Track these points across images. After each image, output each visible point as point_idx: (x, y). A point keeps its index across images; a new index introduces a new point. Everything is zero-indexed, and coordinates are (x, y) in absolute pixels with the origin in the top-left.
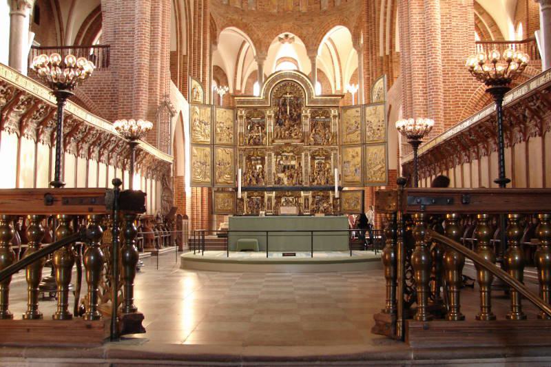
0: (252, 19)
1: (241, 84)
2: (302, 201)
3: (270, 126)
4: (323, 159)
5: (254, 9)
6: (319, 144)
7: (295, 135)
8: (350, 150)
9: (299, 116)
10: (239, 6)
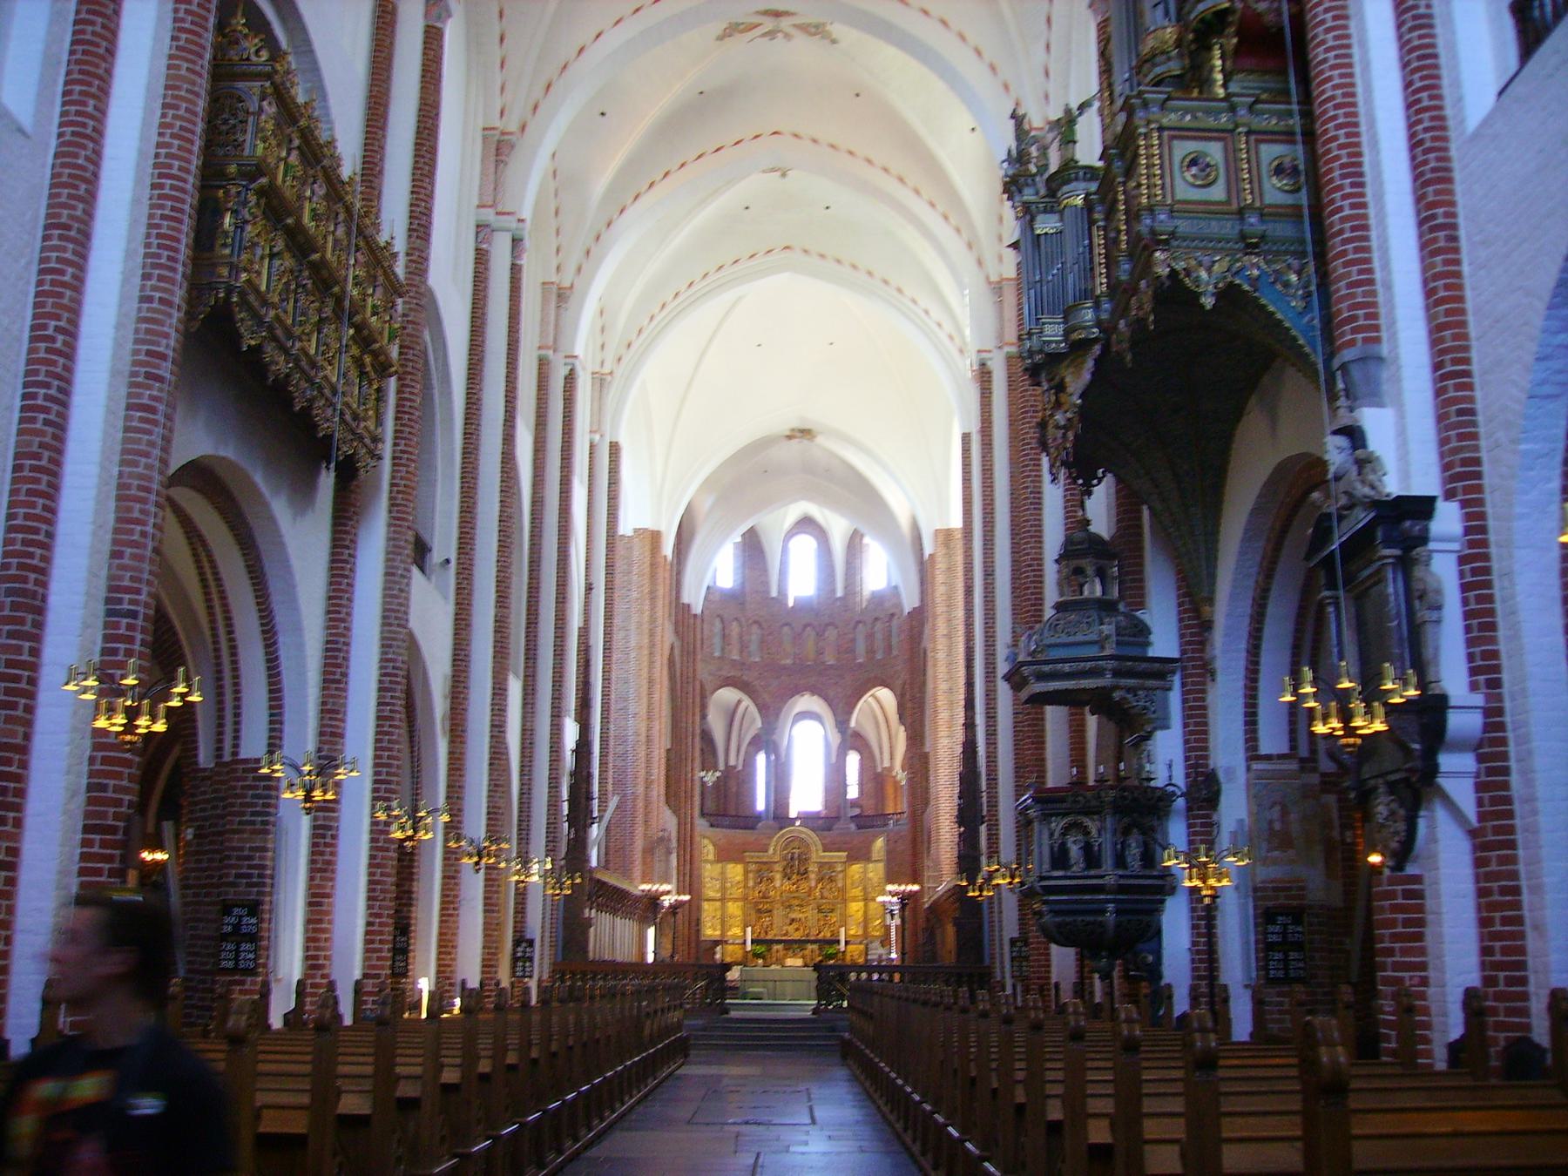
1: (738, 755)
3: (778, 883)
5: (757, 660)
9: (806, 872)
10: (736, 657)
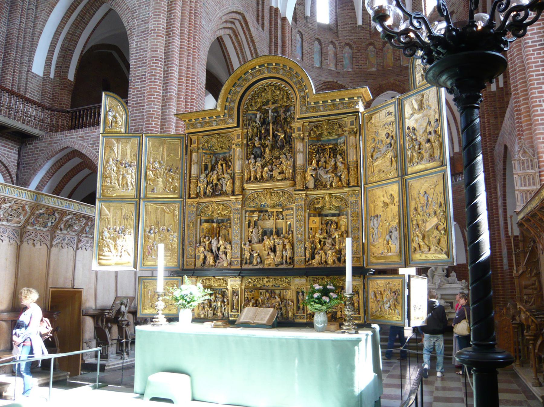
0: (349, 80)
2: (290, 294)
4: (334, 215)
5: (350, 70)
6: (325, 186)
7: (282, 172)
8: (379, 192)
